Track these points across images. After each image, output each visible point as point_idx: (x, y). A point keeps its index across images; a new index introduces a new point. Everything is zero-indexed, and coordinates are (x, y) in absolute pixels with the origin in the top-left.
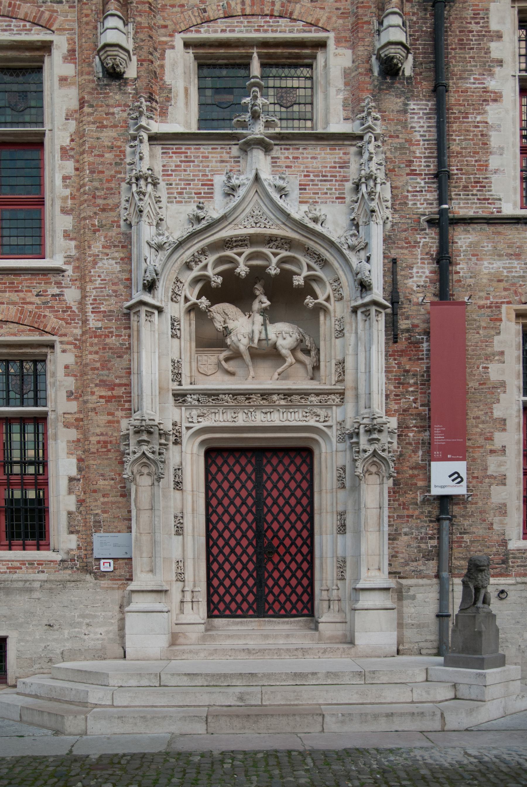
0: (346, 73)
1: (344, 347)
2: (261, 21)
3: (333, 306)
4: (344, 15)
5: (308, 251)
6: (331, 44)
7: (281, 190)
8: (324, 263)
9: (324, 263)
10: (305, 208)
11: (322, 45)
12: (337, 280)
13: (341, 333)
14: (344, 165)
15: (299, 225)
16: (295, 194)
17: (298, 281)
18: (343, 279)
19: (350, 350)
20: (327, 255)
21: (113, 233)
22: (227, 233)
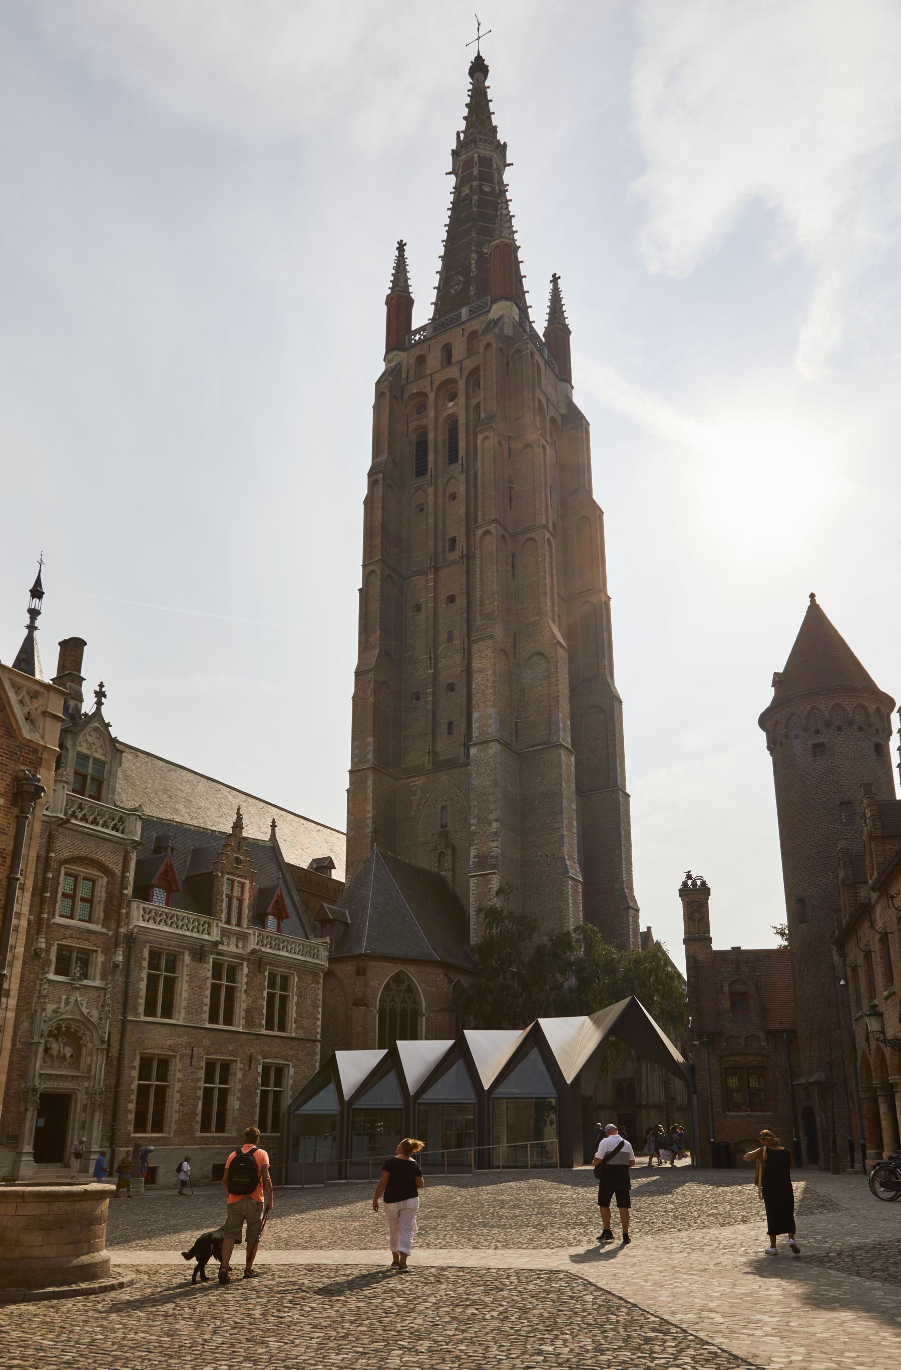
0: (102, 963)
1: (92, 1060)
2: (80, 941)
3: (90, 1045)
4: (104, 943)
5: (84, 1024)
6: (99, 952)
7: (82, 1004)
8: (88, 1029)
9: (88, 1029)
10: (87, 1011)
11: (97, 951)
12: (92, 1037)
13: (91, 1055)
14: (99, 996)
15: (86, 1017)
16: (85, 1005)
17: (80, 1034)
18: (95, 1036)
19: (94, 1062)
20: (90, 1026)
21: (29, 1013)
22: (63, 1017)
